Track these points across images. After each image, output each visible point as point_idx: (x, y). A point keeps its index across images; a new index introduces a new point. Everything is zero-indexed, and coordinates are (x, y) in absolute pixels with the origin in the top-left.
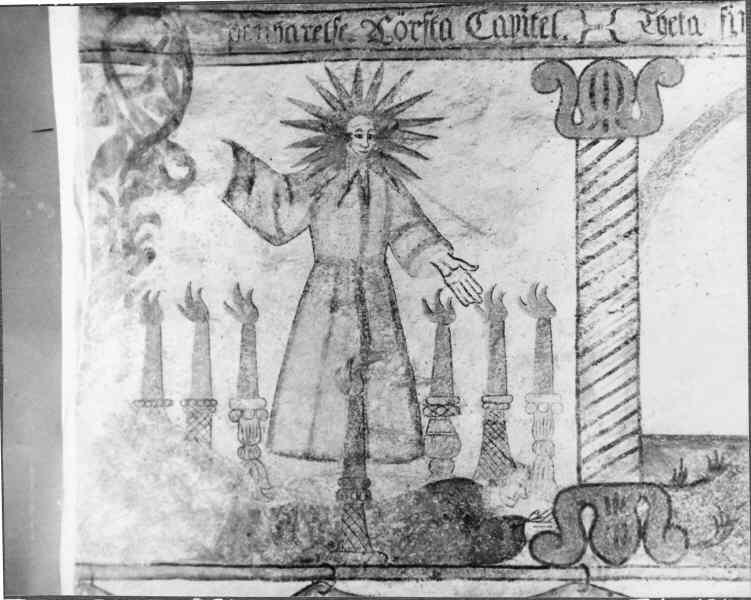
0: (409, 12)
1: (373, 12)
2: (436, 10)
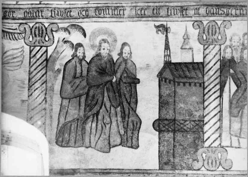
0: (151, 174)
1: (140, 174)
2: (159, 174)
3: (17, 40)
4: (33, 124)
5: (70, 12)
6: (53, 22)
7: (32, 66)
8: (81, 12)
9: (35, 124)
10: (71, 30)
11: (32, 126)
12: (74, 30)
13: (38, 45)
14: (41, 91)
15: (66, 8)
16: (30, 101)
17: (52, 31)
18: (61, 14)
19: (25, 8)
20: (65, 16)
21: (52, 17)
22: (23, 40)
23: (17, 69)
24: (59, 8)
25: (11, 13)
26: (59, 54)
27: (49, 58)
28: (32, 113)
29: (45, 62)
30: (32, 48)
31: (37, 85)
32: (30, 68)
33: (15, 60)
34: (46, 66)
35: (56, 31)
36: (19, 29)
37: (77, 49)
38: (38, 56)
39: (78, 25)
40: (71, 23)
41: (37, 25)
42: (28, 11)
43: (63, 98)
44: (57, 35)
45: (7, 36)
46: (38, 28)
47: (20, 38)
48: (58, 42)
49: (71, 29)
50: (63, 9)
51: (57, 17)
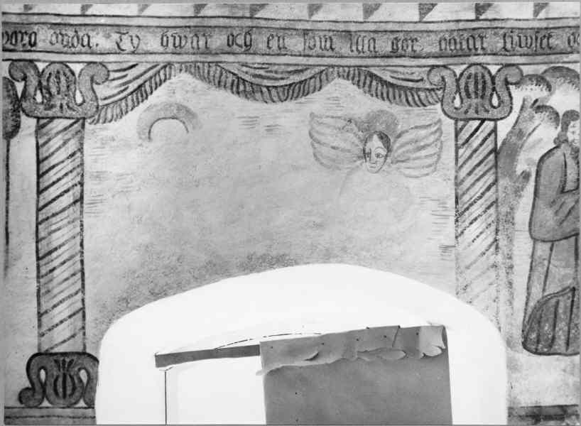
3: (424, 105)
4: (471, 302)
5: (548, 39)
6: (509, 62)
7: (461, 166)
8: (575, 38)
9: (475, 302)
10: (553, 80)
11: (468, 306)
12: (558, 80)
13: (476, 116)
14: (484, 225)
15: (538, 28)
16: (460, 248)
17: (507, 83)
18: (527, 44)
19: (442, 31)
20: (536, 46)
21: (506, 50)
22: (439, 105)
23: (427, 174)
24: (522, 29)
25: (410, 41)
26: (525, 138)
27: (501, 147)
28: (470, 275)
29: (492, 157)
30: (460, 124)
31: (476, 210)
32: (457, 172)
33: (423, 153)
34: (496, 165)
35: (517, 84)
36: (428, 79)
37: (568, 125)
38: (475, 142)
39: (568, 69)
40: (552, 63)
41: (473, 70)
42: (448, 39)
43: (535, 240)
44: (518, 95)
45: (400, 96)
46: (473, 76)
47: (431, 100)
48: (521, 110)
49: (553, 77)
50: (532, 31)
51: (518, 51)
